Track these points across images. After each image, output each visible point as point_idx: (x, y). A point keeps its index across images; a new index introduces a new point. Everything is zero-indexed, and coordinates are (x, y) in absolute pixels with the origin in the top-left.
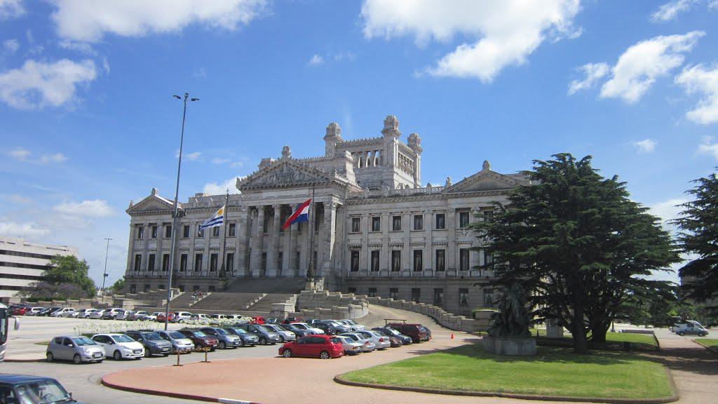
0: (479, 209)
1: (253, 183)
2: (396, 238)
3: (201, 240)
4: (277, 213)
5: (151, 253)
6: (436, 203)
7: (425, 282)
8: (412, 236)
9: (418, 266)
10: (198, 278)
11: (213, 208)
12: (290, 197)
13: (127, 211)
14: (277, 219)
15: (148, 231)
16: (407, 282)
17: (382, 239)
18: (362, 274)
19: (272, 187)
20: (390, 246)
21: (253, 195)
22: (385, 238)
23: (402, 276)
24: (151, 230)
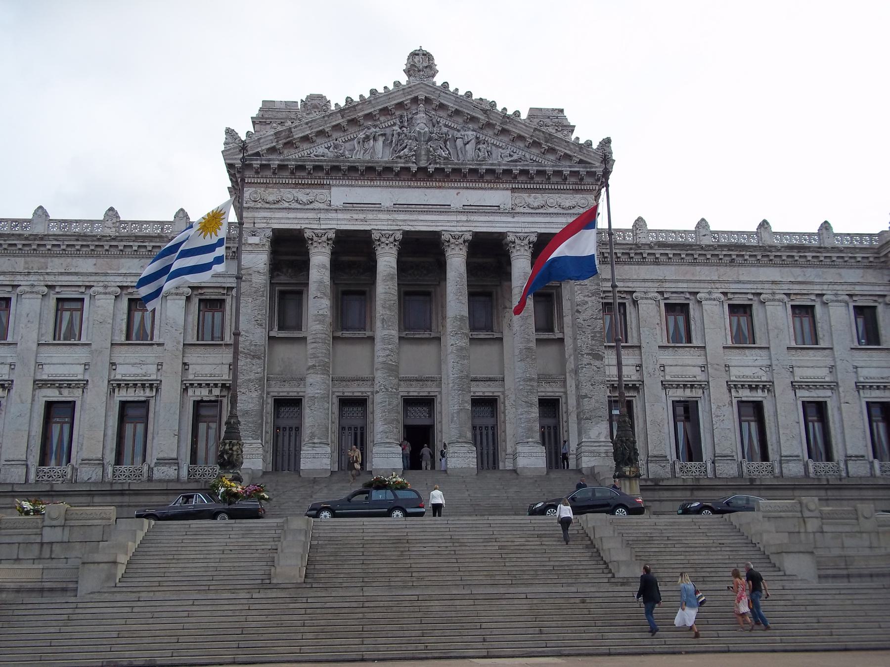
1: (292, 156)
2: (747, 365)
4: (387, 261)
6: (852, 275)
7: (855, 493)
8: (794, 364)
9: (821, 447)
11: (56, 237)
12: (444, 209)
14: (389, 277)
17: (704, 368)
18: (656, 470)
20: (732, 386)
21: (288, 194)
22: (715, 363)
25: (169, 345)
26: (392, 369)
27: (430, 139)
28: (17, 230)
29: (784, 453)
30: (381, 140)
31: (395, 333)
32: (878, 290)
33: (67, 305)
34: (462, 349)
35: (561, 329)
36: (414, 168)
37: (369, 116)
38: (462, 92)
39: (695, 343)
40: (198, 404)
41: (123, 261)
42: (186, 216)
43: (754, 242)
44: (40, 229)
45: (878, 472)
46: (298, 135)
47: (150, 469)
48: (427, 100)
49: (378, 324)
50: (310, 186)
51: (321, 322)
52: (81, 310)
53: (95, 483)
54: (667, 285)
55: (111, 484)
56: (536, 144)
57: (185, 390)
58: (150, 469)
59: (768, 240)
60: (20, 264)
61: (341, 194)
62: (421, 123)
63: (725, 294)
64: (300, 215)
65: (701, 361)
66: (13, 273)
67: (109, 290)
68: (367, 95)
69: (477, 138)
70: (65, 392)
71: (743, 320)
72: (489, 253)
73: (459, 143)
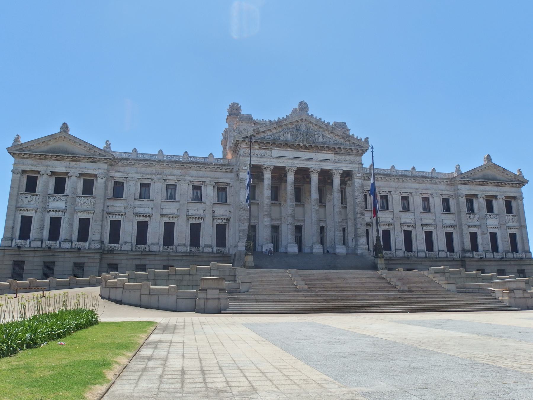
0: (485, 197)
2: (407, 218)
3: (145, 202)
5: (53, 214)
6: (442, 187)
10: (143, 254)
12: (311, 159)
13: (8, 149)
15: (45, 184)
16: (423, 263)
19: (286, 145)
23: (418, 257)
24: (52, 182)
25: (208, 203)
26: (293, 217)
27: (307, 135)
28: (152, 158)
29: (419, 249)
30: (290, 133)
31: (294, 204)
32: (450, 193)
33: (170, 187)
34: (317, 210)
35: (346, 204)
36: (302, 144)
37: (286, 125)
38: (318, 118)
39: (390, 208)
40: (218, 225)
41: (190, 171)
42: (213, 156)
43: (410, 174)
44: (160, 158)
45: (449, 256)
46: (261, 130)
47: (203, 248)
48: (306, 120)
49: (288, 201)
50: (265, 149)
51: (269, 199)
52: (175, 189)
53: (184, 253)
54: (381, 188)
55: (190, 253)
56: (343, 138)
57: (213, 220)
58: (203, 248)
59: (415, 174)
60: (154, 170)
61: (276, 152)
62: (303, 128)
63: (400, 192)
64: (261, 159)
65: (392, 216)
66: (152, 174)
67: (186, 182)
68: (285, 117)
69: (323, 135)
70: (171, 219)
71: (405, 202)
72: (326, 176)
73: (316, 136)
